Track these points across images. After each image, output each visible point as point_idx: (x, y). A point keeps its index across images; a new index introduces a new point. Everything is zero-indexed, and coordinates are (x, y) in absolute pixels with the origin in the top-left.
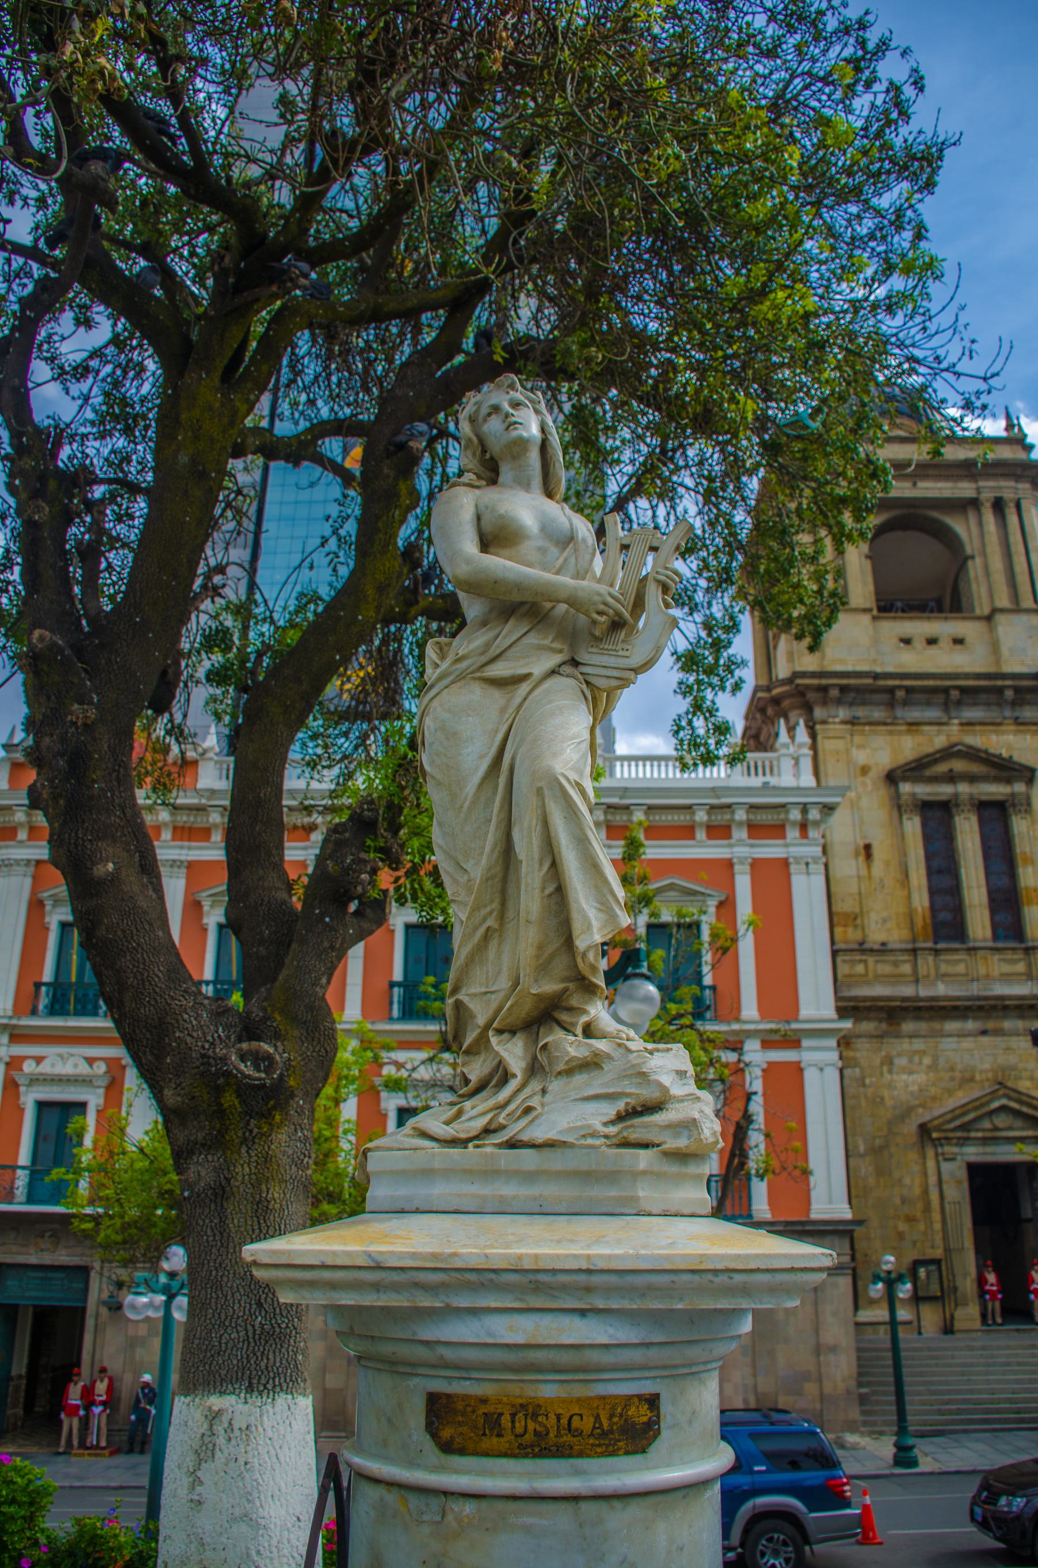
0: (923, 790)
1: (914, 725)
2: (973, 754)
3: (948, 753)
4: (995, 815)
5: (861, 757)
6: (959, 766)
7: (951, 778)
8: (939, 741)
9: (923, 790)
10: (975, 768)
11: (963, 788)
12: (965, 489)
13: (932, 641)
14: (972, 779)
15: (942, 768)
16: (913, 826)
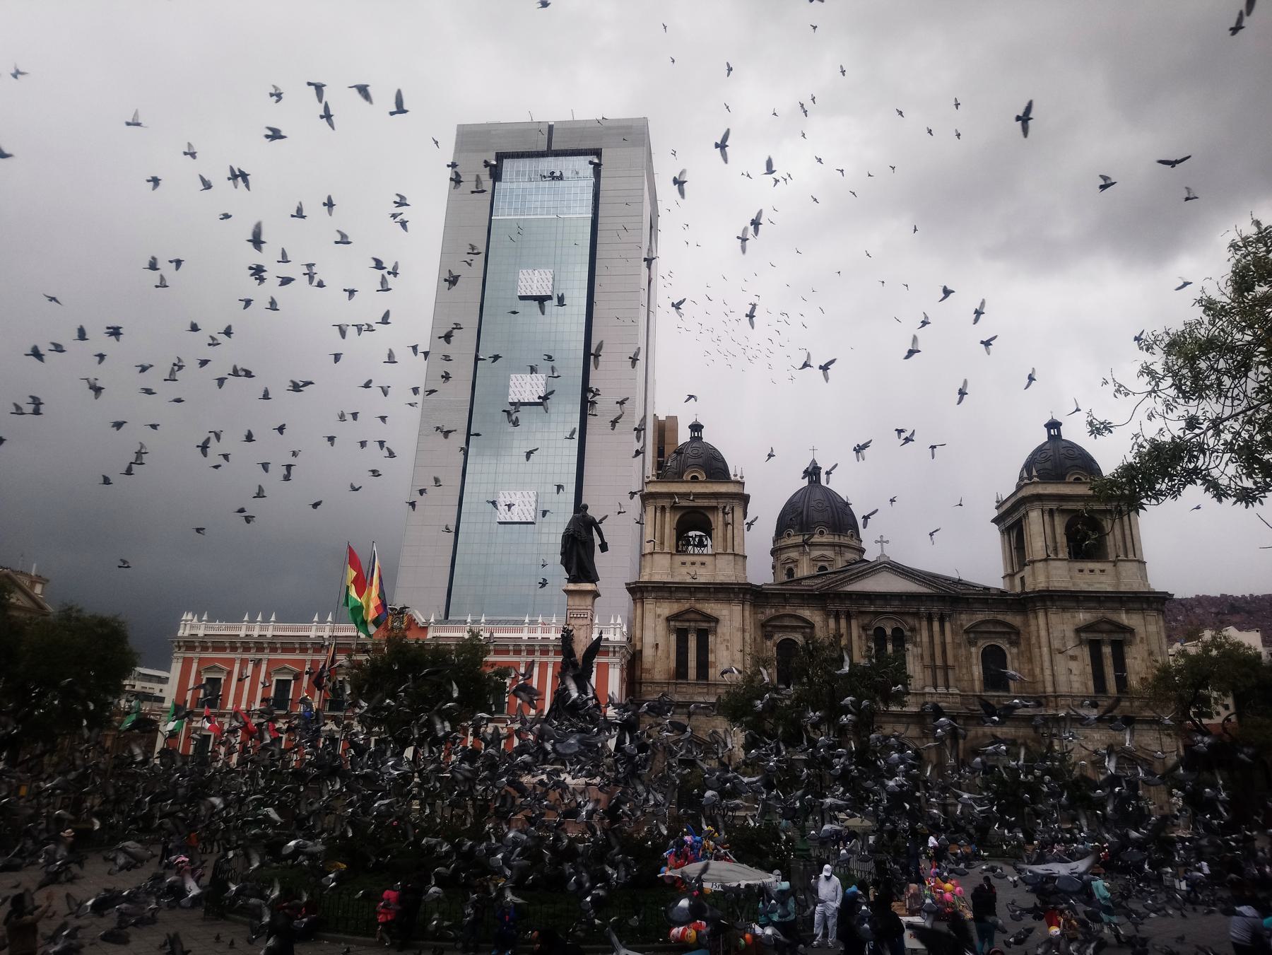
0: (678, 624)
1: (678, 600)
2: (697, 612)
3: (687, 611)
4: (703, 636)
5: (659, 611)
6: (692, 616)
7: (689, 621)
8: (687, 606)
9: (678, 624)
10: (698, 617)
11: (692, 624)
12: (713, 503)
13: (693, 564)
14: (696, 621)
15: (686, 617)
16: (673, 638)
